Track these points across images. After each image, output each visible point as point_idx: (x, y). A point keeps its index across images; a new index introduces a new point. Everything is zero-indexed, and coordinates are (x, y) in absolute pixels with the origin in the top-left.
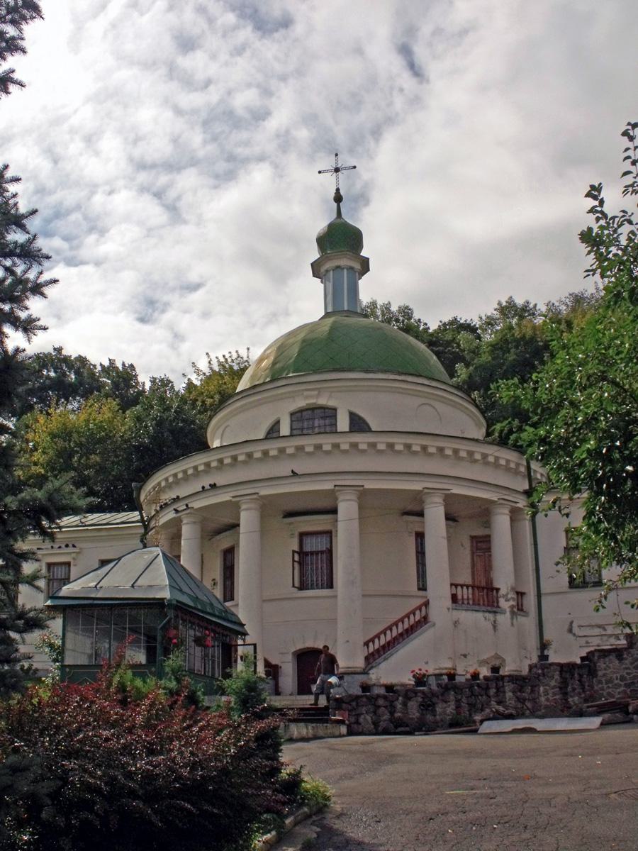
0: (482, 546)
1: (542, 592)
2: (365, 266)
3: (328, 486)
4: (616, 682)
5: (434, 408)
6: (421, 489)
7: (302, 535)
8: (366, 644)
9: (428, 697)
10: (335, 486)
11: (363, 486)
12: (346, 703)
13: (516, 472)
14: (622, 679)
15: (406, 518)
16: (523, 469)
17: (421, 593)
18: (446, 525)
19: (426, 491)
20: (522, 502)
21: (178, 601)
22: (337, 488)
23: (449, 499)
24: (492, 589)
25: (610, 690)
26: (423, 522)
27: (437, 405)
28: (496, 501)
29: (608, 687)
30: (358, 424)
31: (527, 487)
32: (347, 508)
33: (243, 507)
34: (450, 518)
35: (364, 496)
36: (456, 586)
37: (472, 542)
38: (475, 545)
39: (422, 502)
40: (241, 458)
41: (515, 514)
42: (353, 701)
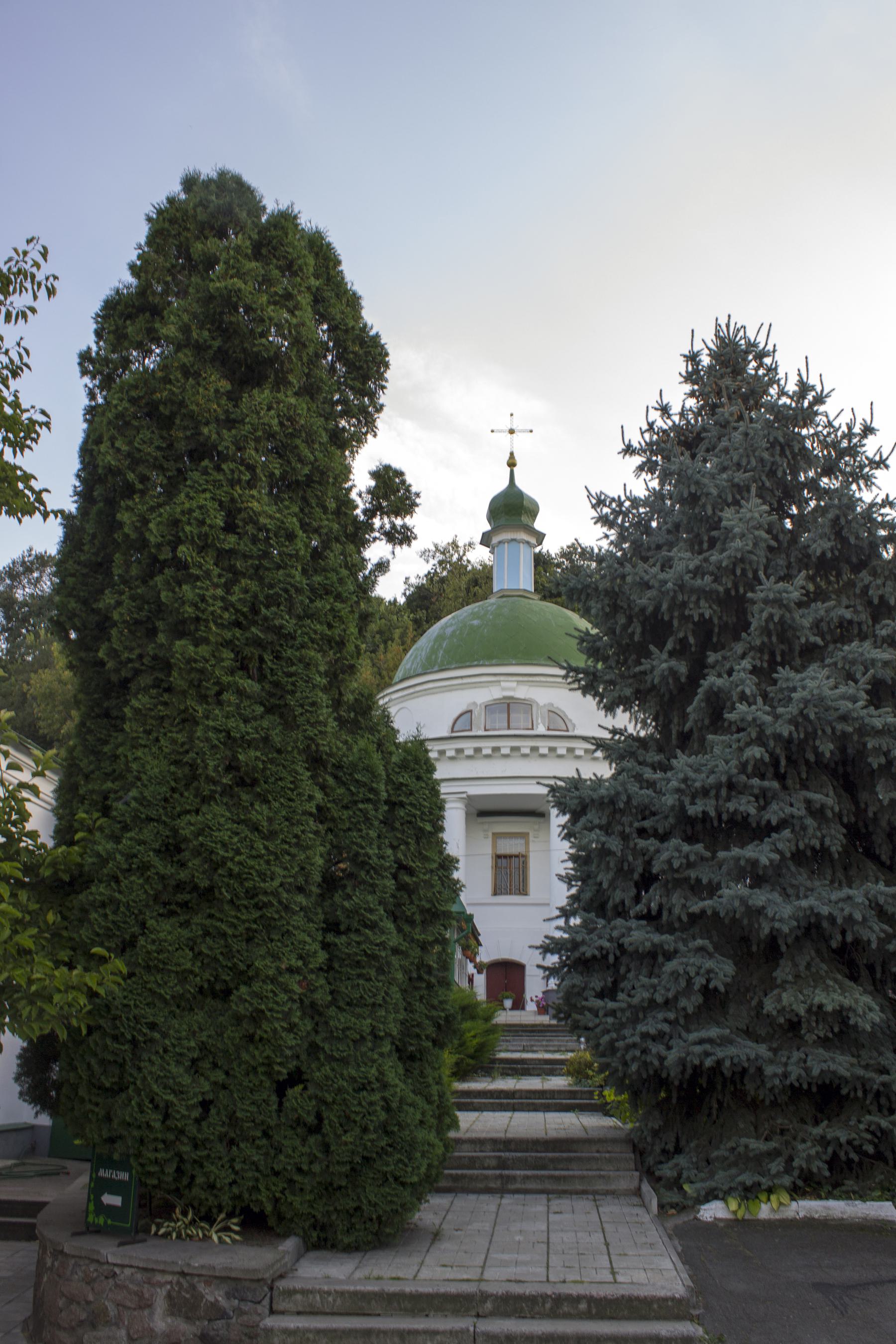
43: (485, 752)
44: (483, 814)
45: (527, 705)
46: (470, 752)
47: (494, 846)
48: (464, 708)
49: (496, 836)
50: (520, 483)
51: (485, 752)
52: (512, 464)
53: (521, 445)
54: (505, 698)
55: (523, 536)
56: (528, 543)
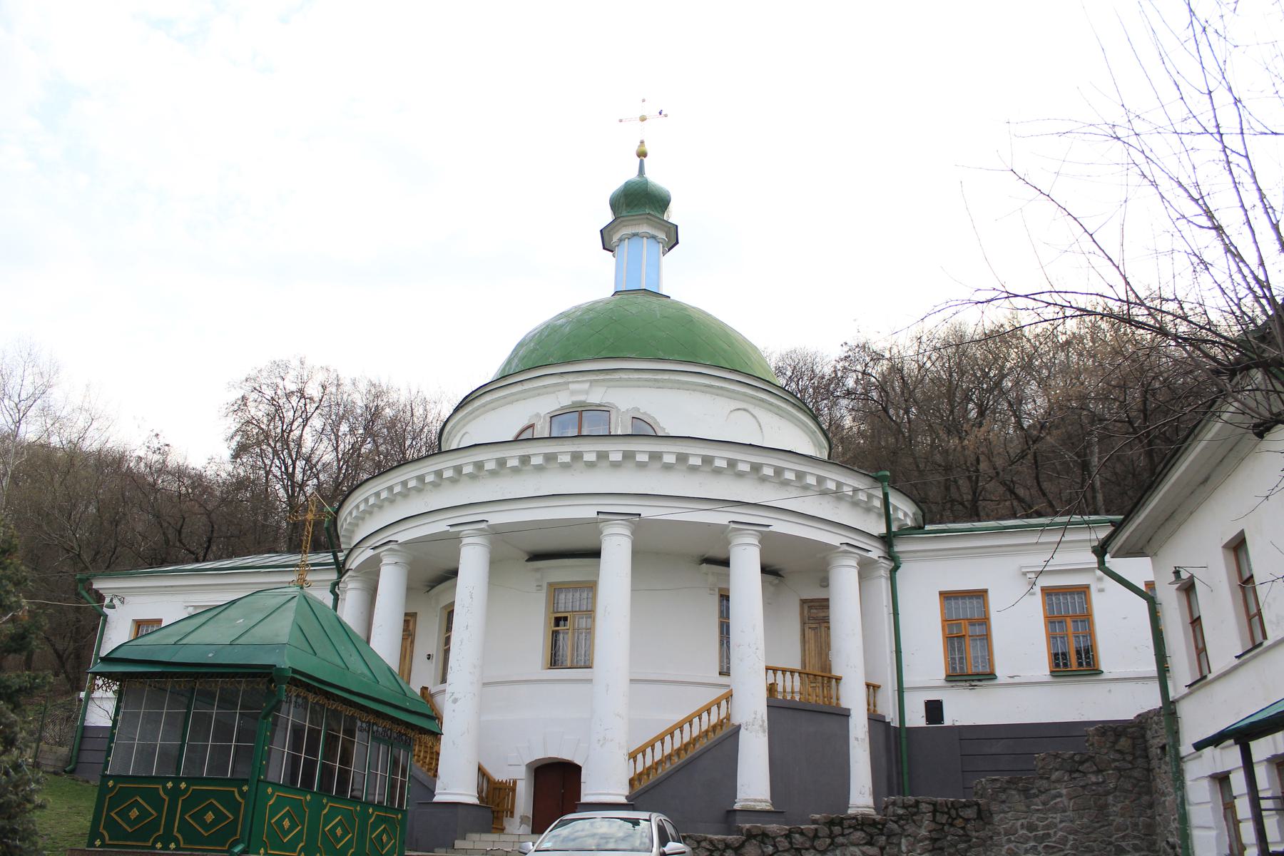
0: (816, 616)
2: (672, 238)
3: (587, 511)
4: (1021, 832)
8: (633, 756)
9: (718, 849)
13: (869, 509)
14: (1031, 828)
16: (877, 503)
17: (724, 680)
18: (763, 582)
20: (876, 552)
21: (295, 671)
22: (601, 516)
23: (768, 541)
24: (830, 678)
25: (1012, 846)
26: (728, 575)
27: (758, 412)
29: (1009, 841)
30: (643, 431)
31: (883, 530)
32: (617, 550)
33: (465, 541)
34: (767, 570)
36: (775, 670)
40: (467, 470)
41: (865, 569)
44: (536, 556)
45: (603, 410)
48: (525, 423)
49: (555, 589)
52: (642, 154)
54: (575, 404)
55: (644, 229)
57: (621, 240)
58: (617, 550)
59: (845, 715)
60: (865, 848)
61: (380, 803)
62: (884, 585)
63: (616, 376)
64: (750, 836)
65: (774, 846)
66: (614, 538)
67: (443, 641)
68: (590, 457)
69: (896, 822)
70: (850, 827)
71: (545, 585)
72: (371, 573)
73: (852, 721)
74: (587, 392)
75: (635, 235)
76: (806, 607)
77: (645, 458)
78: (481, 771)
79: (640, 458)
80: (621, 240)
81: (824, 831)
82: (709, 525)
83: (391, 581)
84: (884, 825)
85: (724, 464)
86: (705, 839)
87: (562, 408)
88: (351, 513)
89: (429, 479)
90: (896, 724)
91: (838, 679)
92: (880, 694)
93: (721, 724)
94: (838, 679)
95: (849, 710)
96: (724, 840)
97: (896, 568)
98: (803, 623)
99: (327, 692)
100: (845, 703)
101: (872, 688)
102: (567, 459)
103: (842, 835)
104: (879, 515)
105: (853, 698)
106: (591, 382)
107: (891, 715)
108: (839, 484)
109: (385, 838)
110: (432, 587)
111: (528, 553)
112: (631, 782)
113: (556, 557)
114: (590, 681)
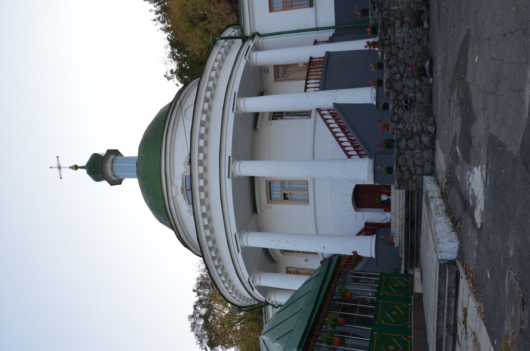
1: (315, 27)
3: (228, 184)
5: (188, 107)
6: (233, 114)
7: (270, 198)
8: (349, 156)
10: (229, 177)
11: (229, 157)
12: (403, 176)
15: (258, 127)
19: (235, 110)
20: (251, 43)
22: (230, 176)
28: (247, 61)
31: (240, 41)
32: (247, 168)
33: (246, 244)
35: (238, 155)
37: (278, 81)
38: (280, 79)
39: (245, 114)
41: (257, 48)
42: (401, 170)
43: (206, 222)
46: (208, 233)
47: (277, 201)
50: (84, 164)
51: (206, 222)
52: (76, 167)
53: (67, 163)
54: (183, 193)
55: (108, 165)
56: (113, 161)
57: (115, 176)
58: (247, 168)
59: (328, 54)
60: (396, 27)
61: (377, 288)
62: (266, 40)
63: (168, 173)
64: (390, 87)
65: (396, 74)
66: (241, 169)
67: (299, 254)
68: (202, 182)
69: (382, 13)
70: (385, 36)
71: (269, 205)
72: (265, 290)
73: (331, 51)
74: (177, 187)
75: (112, 169)
76: (277, 79)
77: (202, 155)
78: (359, 234)
79: (201, 158)
80: (115, 176)
81: (387, 49)
82: (235, 123)
83: (268, 280)
84: (384, 19)
85: (204, 116)
86: (393, 110)
87: (185, 199)
88: (238, 301)
89: (217, 263)
90: (333, 31)
91: (311, 58)
92: (318, 40)
93: (334, 115)
94: (311, 58)
95: (326, 52)
96: (393, 101)
97: (258, 34)
98: (286, 80)
99: (314, 323)
100: (323, 54)
101: (316, 43)
102: (203, 194)
103: (389, 39)
104: (233, 43)
105: (319, 52)
106: (171, 185)
107: (330, 33)
108: (216, 60)
109: (396, 285)
110: (274, 260)
111: (253, 214)
112: (361, 156)
113: (252, 199)
114: (314, 179)
